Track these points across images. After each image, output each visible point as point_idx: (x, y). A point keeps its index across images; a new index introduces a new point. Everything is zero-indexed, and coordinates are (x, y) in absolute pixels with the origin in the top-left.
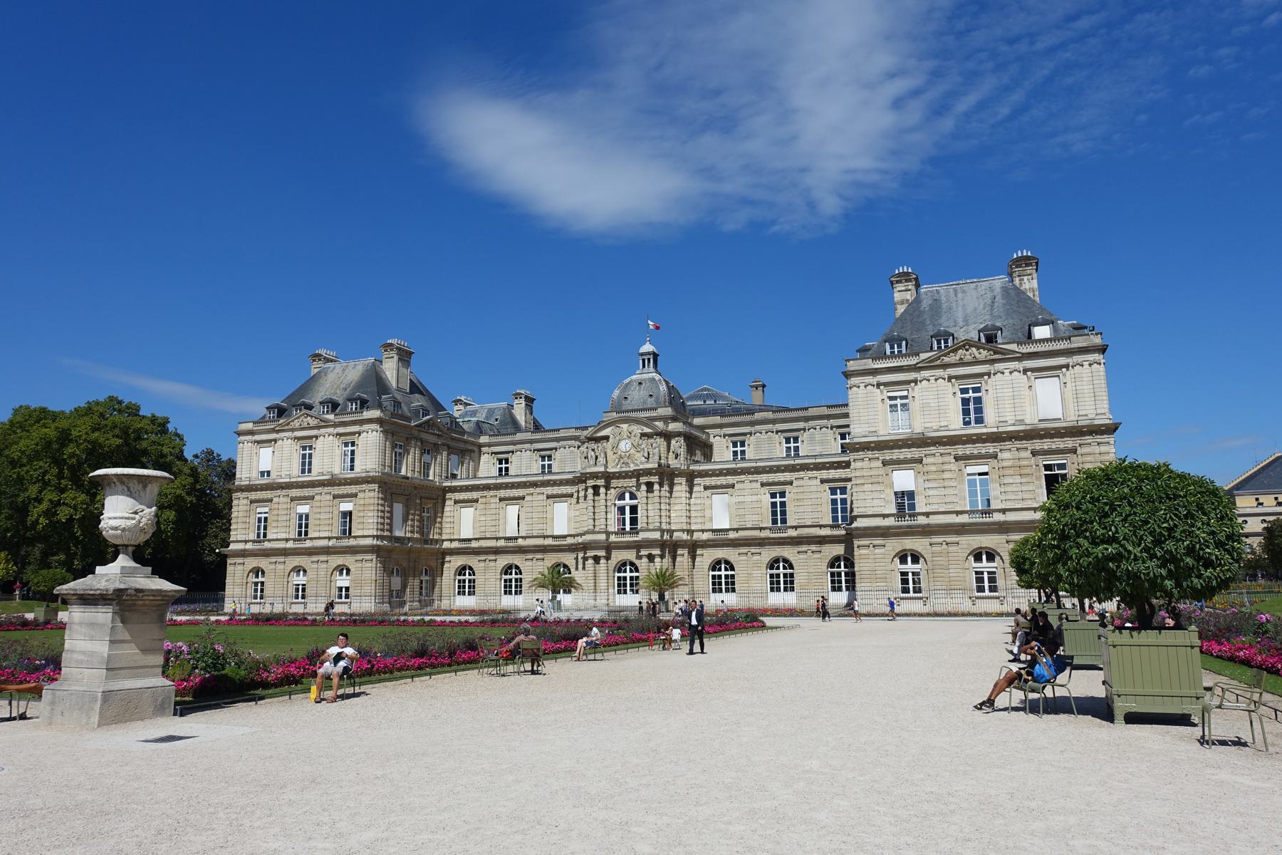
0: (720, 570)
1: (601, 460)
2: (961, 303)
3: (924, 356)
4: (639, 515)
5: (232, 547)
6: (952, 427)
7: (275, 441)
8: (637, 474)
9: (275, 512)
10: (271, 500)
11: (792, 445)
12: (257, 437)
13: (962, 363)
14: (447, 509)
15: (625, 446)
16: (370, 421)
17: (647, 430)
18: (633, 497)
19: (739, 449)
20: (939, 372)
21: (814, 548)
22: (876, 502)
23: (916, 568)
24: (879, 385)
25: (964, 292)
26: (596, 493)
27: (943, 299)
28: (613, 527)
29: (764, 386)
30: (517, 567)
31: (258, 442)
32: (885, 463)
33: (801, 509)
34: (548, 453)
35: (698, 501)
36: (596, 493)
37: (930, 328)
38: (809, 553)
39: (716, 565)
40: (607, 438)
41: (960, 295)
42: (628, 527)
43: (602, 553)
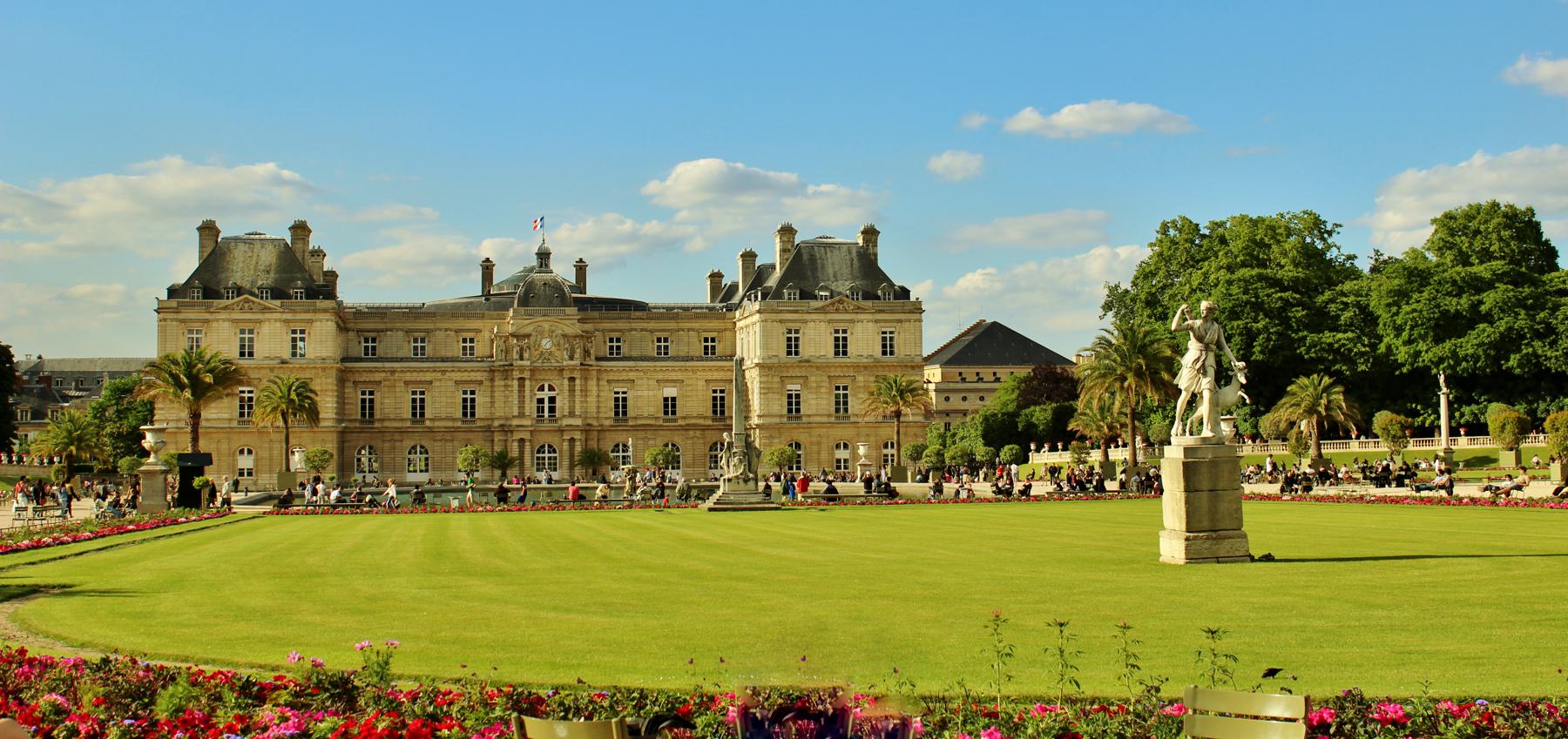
1: (526, 355)
4: (558, 404)
7: (207, 321)
8: (562, 370)
12: (181, 316)
15: (546, 344)
16: (325, 311)
17: (569, 331)
18: (551, 388)
20: (822, 317)
21: (698, 433)
24: (781, 321)
31: (183, 321)
39: (616, 448)
40: (528, 336)
42: (546, 414)
43: (527, 436)
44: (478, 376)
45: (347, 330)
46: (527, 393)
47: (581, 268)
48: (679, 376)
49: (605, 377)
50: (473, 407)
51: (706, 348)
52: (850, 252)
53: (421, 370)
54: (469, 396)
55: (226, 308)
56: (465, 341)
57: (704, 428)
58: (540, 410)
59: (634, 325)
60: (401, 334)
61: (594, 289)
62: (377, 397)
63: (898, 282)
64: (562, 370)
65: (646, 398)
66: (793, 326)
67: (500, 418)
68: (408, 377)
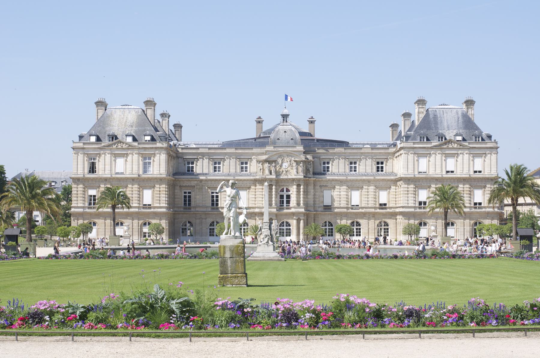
2: (445, 118)
3: (434, 144)
5: (73, 210)
7: (99, 154)
14: (176, 191)
25: (447, 113)
27: (439, 116)
37: (434, 128)
40: (275, 161)
41: (445, 114)
42: (285, 204)
45: (178, 157)
46: (274, 193)
51: (378, 168)
52: (457, 113)
55: (109, 146)
56: (242, 163)
61: (318, 135)
62: (192, 195)
63: (485, 132)
67: (258, 208)
68: (209, 184)
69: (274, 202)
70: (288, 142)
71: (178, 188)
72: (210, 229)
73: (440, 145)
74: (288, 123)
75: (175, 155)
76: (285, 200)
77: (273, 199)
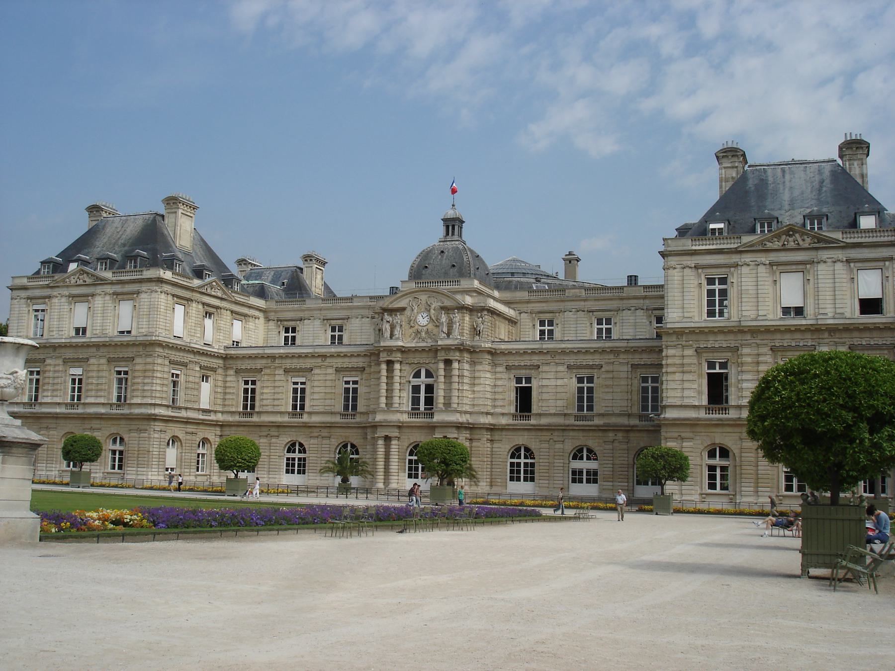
0: (519, 457)
1: (397, 332)
2: (788, 184)
6: (770, 317)
7: (49, 297)
8: (434, 351)
9: (47, 375)
10: (44, 360)
11: (604, 326)
13: (784, 249)
14: (229, 379)
15: (423, 320)
17: (448, 303)
18: (429, 375)
19: (546, 328)
21: (620, 435)
22: (686, 393)
23: (724, 463)
26: (390, 370)
27: (770, 179)
28: (407, 406)
29: (578, 260)
30: (301, 445)
32: (698, 351)
33: (609, 396)
34: (339, 322)
35: (499, 383)
36: (390, 370)
38: (616, 444)
40: (404, 309)
41: (787, 177)
42: (422, 407)
43: (394, 433)
44: (359, 362)
47: (571, 260)
48: (596, 360)
49: (501, 360)
50: (355, 399)
52: (820, 172)
53: (300, 356)
54: (351, 386)
57: (628, 430)
58: (415, 401)
59: (569, 305)
60: (318, 323)
62: (258, 386)
64: (437, 350)
65: (555, 389)
66: (717, 273)
68: (288, 364)
69: (396, 400)
70: (446, 274)
71: (231, 372)
72: (288, 459)
73: (762, 243)
74: (456, 237)
75: (257, 313)
76: (422, 395)
77: (396, 393)
